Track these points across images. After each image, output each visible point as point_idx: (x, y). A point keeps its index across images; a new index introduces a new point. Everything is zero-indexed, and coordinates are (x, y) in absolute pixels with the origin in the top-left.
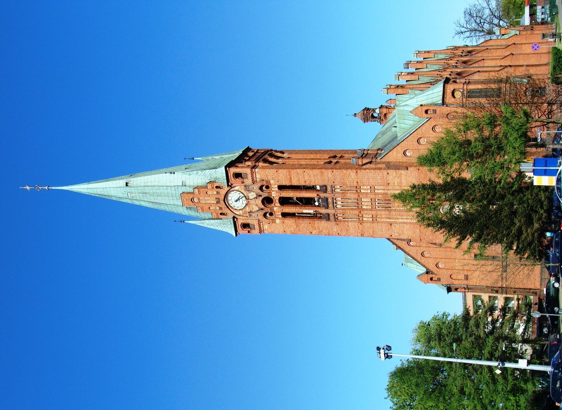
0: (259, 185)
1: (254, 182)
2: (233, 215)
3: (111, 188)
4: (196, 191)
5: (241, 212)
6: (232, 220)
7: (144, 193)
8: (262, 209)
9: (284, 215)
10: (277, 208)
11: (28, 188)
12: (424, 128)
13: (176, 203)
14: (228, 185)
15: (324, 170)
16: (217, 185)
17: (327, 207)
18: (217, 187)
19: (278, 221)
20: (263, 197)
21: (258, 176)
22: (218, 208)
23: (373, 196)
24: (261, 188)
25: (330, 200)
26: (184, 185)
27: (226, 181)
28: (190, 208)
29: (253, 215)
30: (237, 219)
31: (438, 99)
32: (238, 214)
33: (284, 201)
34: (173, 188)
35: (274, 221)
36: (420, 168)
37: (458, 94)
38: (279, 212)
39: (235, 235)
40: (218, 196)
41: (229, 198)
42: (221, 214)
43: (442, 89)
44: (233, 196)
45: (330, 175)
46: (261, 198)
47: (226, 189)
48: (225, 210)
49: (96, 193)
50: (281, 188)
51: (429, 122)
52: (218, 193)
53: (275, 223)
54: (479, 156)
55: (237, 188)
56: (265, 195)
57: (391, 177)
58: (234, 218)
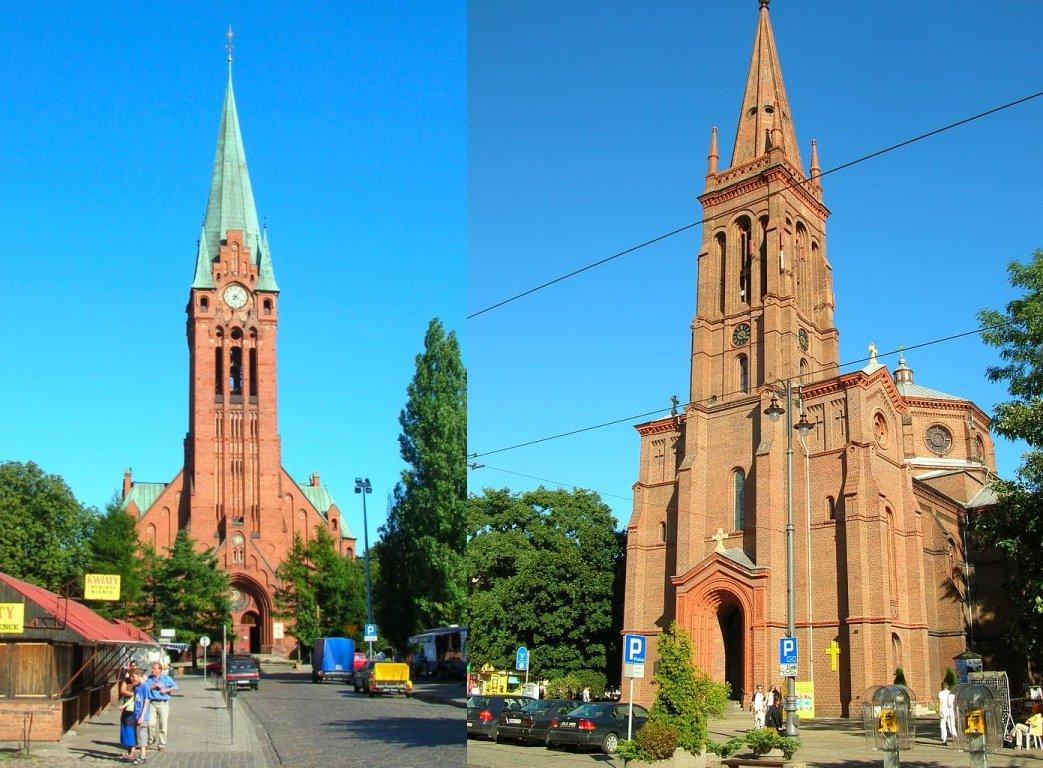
0: (257, 327)
1: (260, 320)
3: (234, 142)
6: (213, 286)
7: (233, 183)
8: (227, 325)
9: (219, 352)
10: (229, 343)
11: (230, 34)
13: (224, 220)
14: (255, 291)
16: (256, 277)
18: (252, 277)
19: (212, 341)
20: (243, 330)
21: (267, 327)
22: (225, 272)
23: (246, 455)
24: (253, 328)
25: (239, 406)
26: (248, 235)
27: (262, 289)
28: (219, 236)
35: (210, 336)
38: (223, 344)
39: (195, 285)
40: (241, 276)
41: (239, 288)
42: (219, 274)
46: (240, 326)
47: (252, 289)
48: (223, 281)
49: (228, 121)
52: (245, 276)
54: (56, 575)
55: (251, 299)
56: (246, 332)
57: (270, 478)
58: (215, 289)
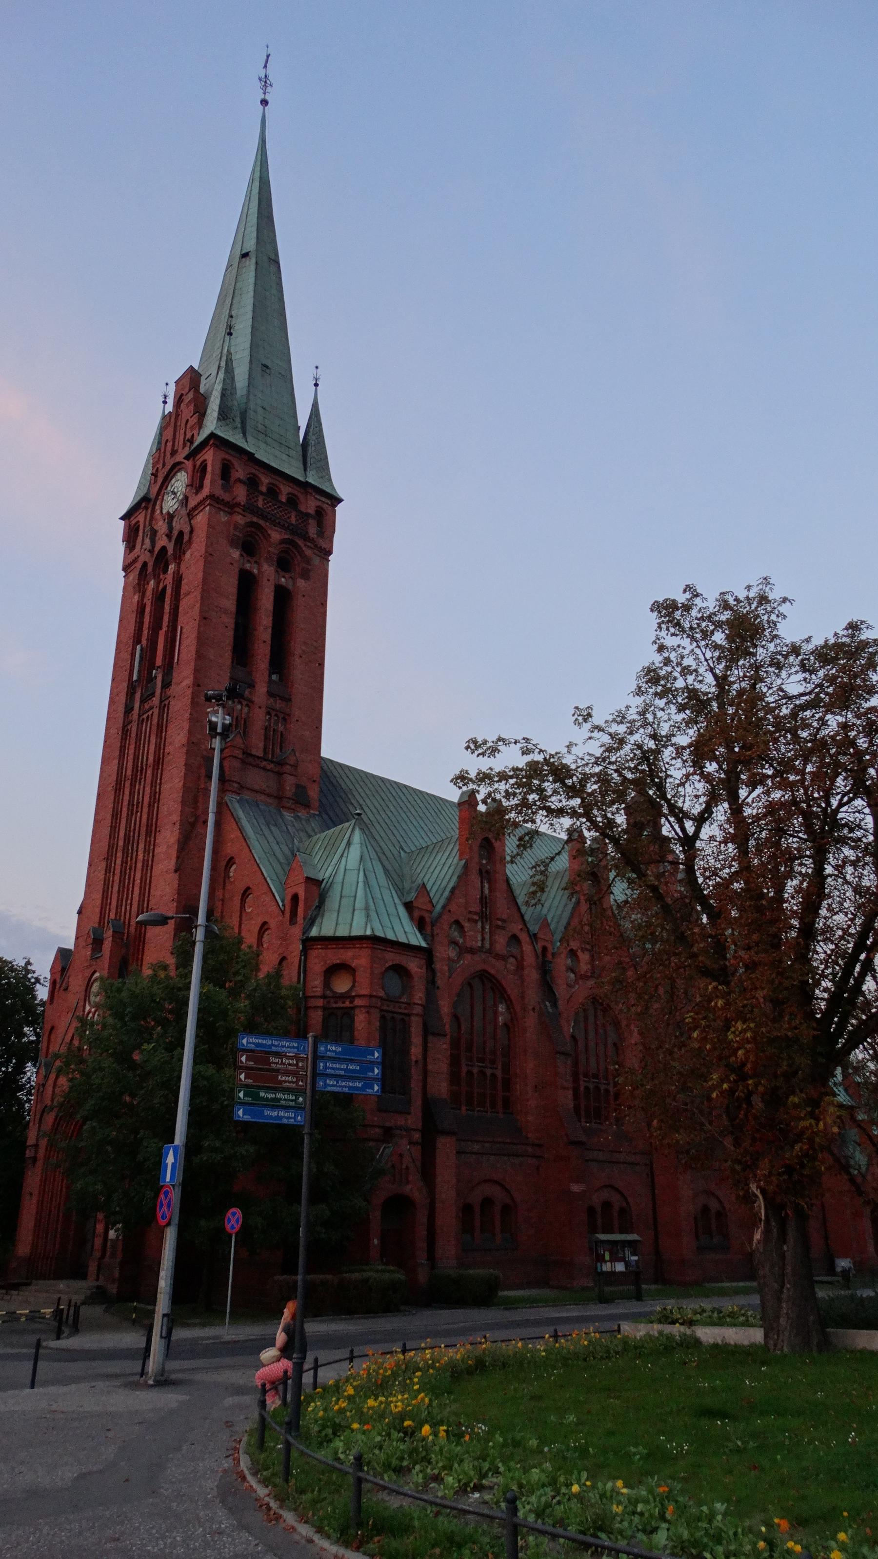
2: (153, 496)
4: (191, 396)
5: (158, 512)
12: (268, 898)
15: (193, 664)
17: (143, 701)
24: (181, 533)
29: (147, 541)
30: (146, 508)
31: (327, 926)
32: (157, 507)
33: (160, 596)
34: (220, 350)
36: (175, 904)
37: (342, 985)
43: (356, 932)
44: (180, 482)
45: (184, 684)
50: (178, 580)
51: (277, 911)
53: (134, 594)
56: (170, 550)
